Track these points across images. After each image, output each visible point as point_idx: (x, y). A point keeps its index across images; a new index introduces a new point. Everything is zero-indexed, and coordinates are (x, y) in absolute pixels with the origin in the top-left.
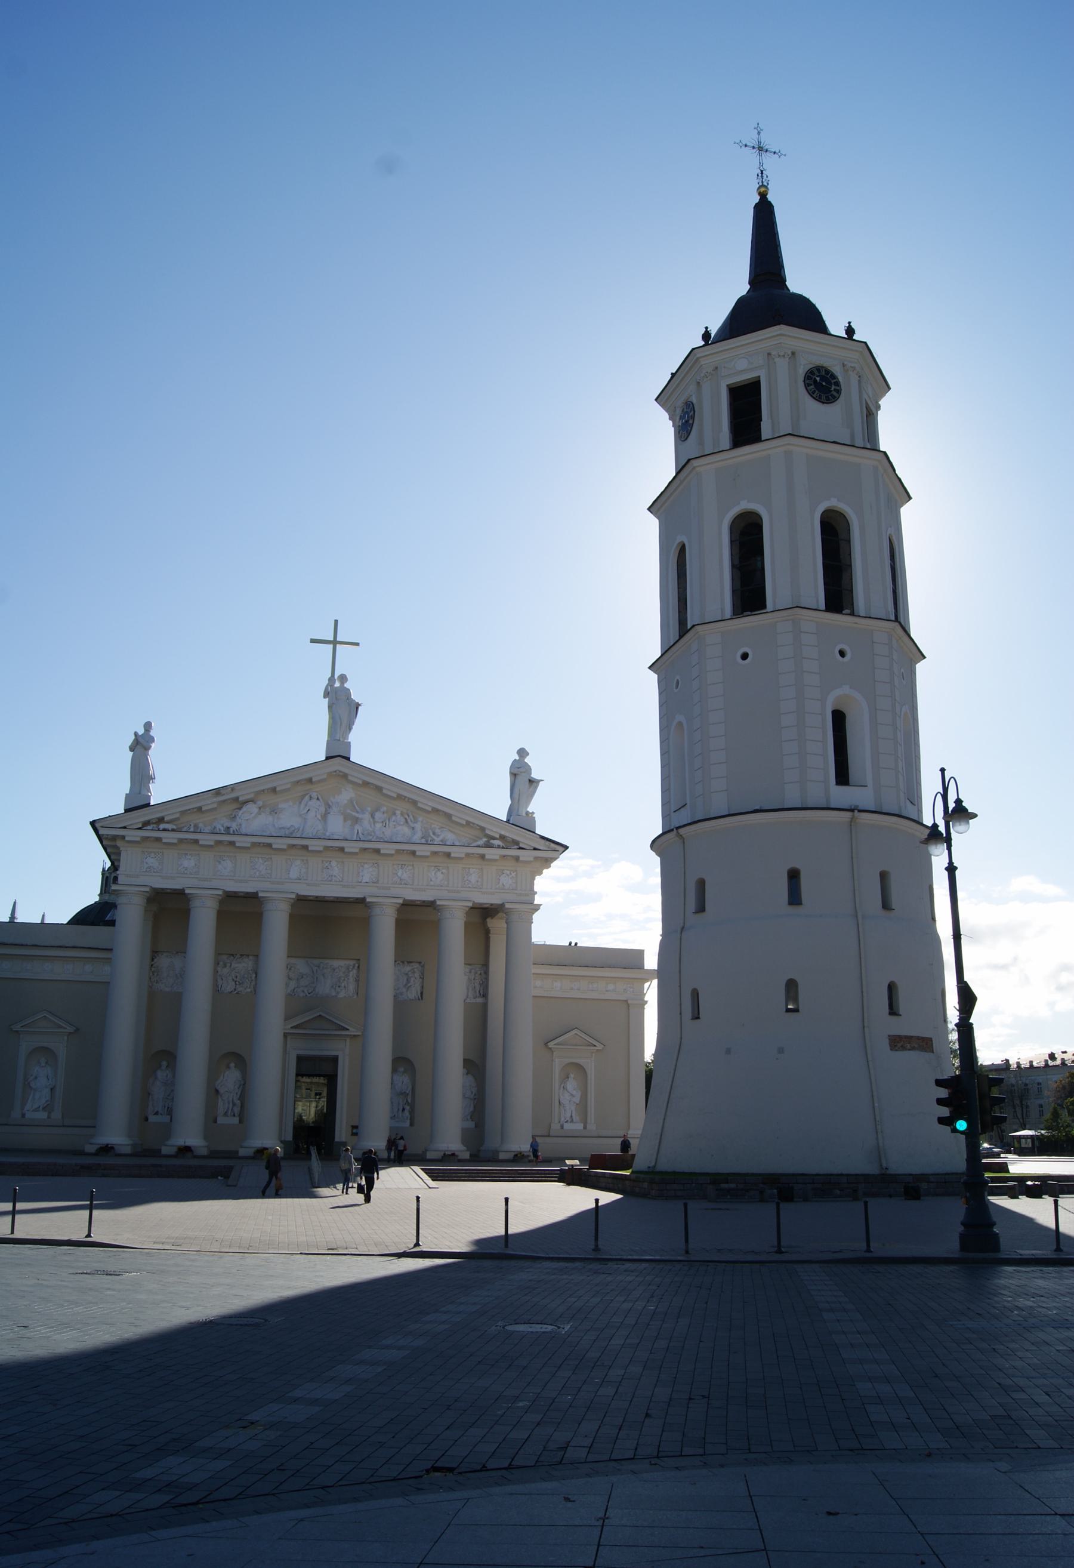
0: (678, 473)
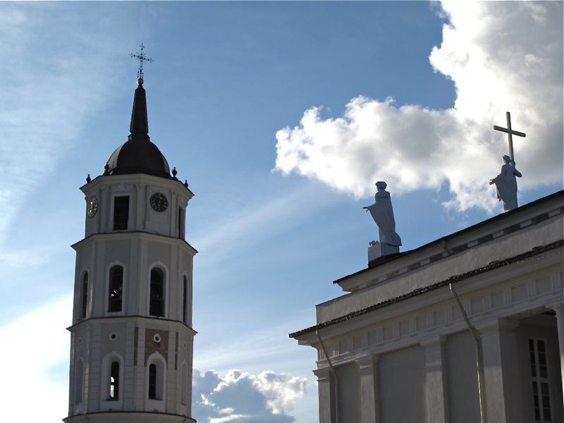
0: (86, 238)
